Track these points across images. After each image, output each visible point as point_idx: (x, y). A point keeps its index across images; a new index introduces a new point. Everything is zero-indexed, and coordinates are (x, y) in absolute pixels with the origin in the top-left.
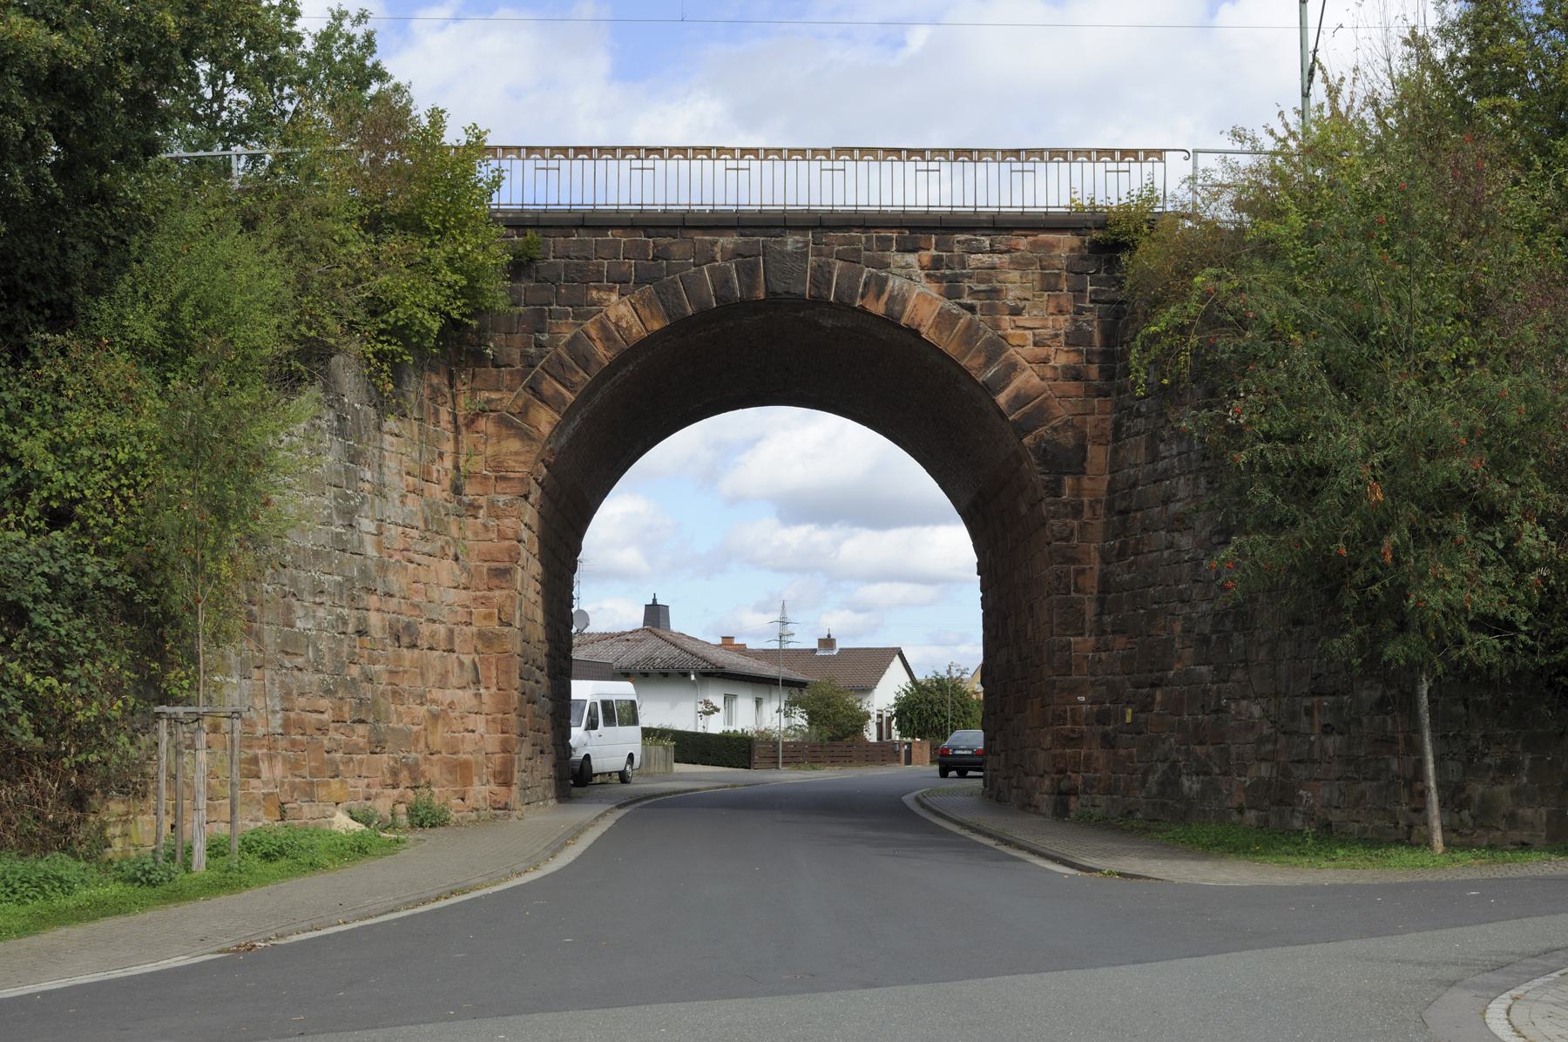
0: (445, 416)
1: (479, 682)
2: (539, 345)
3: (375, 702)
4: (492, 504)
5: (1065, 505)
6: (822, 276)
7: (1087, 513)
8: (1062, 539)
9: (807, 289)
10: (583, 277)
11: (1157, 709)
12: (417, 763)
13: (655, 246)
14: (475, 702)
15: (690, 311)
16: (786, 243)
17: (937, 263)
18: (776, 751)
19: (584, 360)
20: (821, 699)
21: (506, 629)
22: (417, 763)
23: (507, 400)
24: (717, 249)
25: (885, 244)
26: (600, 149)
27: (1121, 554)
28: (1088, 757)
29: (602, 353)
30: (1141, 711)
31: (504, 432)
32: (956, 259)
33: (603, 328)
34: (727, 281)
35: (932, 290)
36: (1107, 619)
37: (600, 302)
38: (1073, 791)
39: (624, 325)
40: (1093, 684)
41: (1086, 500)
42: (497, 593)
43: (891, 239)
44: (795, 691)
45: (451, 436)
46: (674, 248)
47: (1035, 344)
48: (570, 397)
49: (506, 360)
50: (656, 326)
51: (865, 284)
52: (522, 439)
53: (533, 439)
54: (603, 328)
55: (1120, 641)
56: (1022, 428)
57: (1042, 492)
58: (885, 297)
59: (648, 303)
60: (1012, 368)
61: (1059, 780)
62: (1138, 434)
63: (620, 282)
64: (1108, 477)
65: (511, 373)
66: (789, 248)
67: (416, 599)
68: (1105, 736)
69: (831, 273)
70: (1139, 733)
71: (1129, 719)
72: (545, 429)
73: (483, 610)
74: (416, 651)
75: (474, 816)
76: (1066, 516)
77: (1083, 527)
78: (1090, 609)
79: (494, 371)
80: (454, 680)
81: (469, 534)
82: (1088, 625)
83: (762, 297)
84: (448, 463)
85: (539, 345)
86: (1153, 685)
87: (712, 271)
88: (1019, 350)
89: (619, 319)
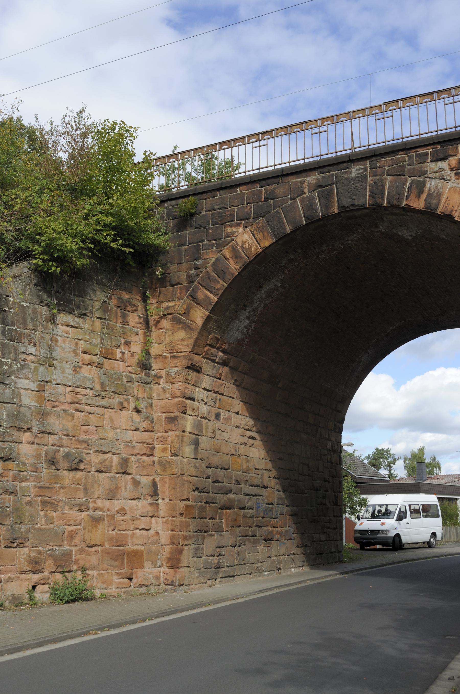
0: (134, 319)
1: (157, 495)
2: (197, 268)
3: (17, 510)
4: (168, 374)
6: (377, 190)
9: (368, 201)
10: (223, 219)
12: (68, 554)
14: (149, 508)
15: (288, 230)
16: (351, 172)
19: (221, 272)
21: (175, 458)
22: (68, 554)
23: (177, 306)
24: (305, 186)
25: (422, 159)
26: (235, 140)
29: (234, 267)
31: (176, 327)
33: (234, 250)
34: (311, 205)
37: (232, 234)
39: (247, 246)
42: (170, 433)
43: (427, 154)
45: (141, 332)
46: (278, 191)
48: (214, 299)
49: (177, 281)
51: (409, 188)
52: (185, 330)
53: (191, 329)
54: (234, 250)
58: (424, 196)
59: (261, 229)
63: (245, 219)
65: (180, 289)
66: (353, 175)
67: (83, 437)
69: (383, 186)
72: (200, 322)
73: (162, 446)
74: (80, 474)
75: (143, 590)
79: (171, 288)
80: (123, 493)
81: (154, 395)
83: (336, 212)
84: (136, 348)
85: (197, 268)
89: (244, 243)
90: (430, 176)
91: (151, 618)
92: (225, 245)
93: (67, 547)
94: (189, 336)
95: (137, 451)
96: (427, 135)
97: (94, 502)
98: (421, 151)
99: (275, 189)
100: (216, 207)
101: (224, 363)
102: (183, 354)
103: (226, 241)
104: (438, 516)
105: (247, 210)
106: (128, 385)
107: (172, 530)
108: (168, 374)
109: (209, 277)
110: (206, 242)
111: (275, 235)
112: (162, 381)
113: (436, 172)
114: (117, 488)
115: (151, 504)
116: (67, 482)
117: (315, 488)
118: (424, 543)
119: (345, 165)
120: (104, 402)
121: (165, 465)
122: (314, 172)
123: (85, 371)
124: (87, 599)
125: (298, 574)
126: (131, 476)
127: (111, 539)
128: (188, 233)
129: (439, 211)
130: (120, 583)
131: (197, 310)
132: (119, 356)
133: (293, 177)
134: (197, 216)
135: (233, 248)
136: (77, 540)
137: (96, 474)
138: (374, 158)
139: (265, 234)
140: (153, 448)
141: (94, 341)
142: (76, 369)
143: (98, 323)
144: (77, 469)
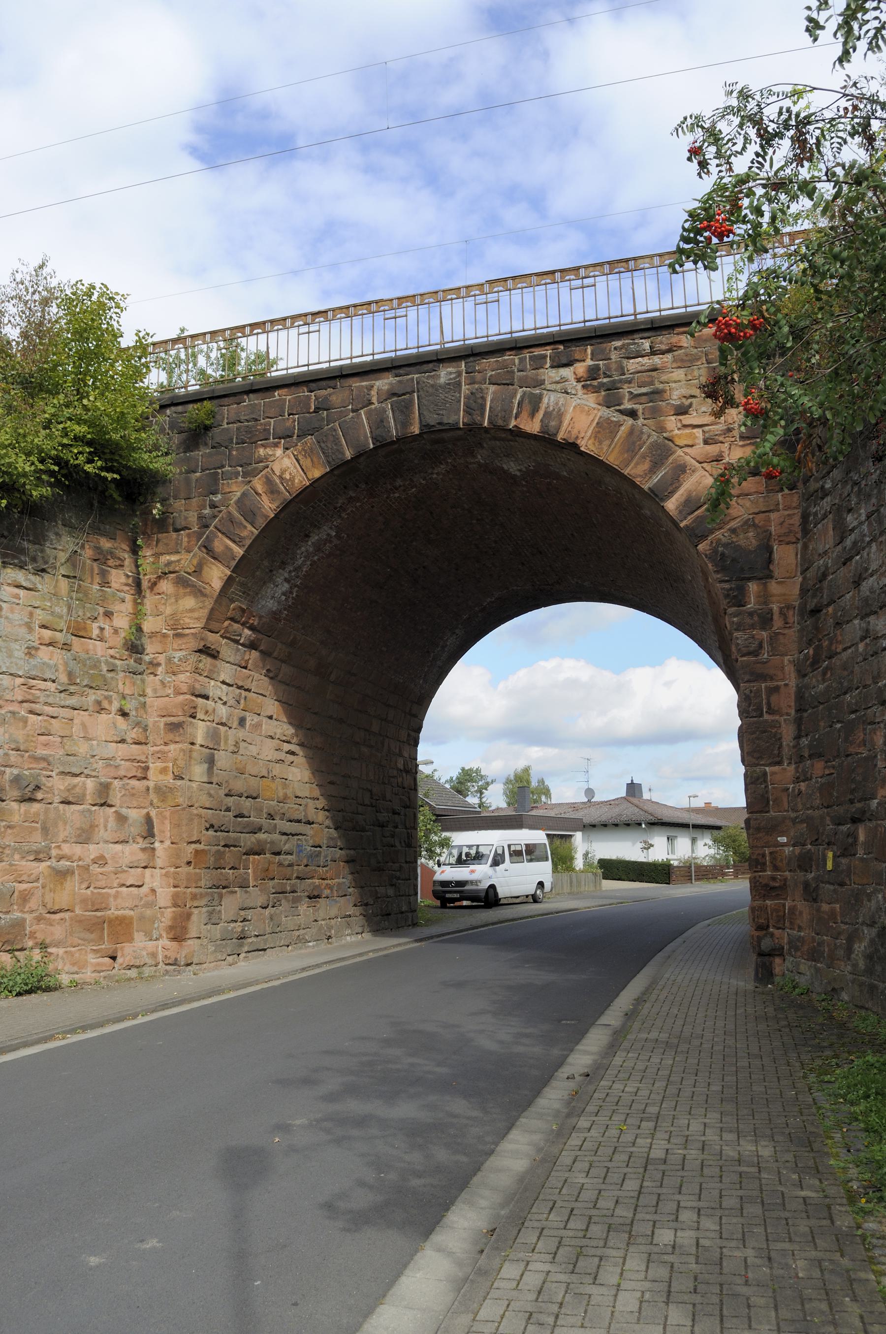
0: (118, 578)
2: (213, 506)
4: (169, 660)
5: (751, 614)
6: (475, 404)
7: (778, 622)
8: (749, 654)
9: (461, 418)
10: (253, 436)
11: (860, 853)
12: (20, 924)
13: (317, 398)
14: (142, 857)
15: (348, 455)
16: (439, 376)
17: (593, 373)
18: (690, 872)
19: (250, 514)
20: (730, 837)
21: (179, 783)
22: (20, 924)
23: (185, 561)
24: (374, 392)
26: (272, 322)
27: (815, 662)
28: (793, 909)
29: (269, 507)
30: (843, 855)
31: (181, 591)
32: (614, 366)
33: (269, 482)
34: (382, 421)
35: (590, 400)
36: (805, 741)
37: (266, 459)
38: (777, 952)
39: (288, 477)
40: (794, 821)
41: (775, 607)
42: (172, 747)
43: (545, 357)
44: (716, 832)
45: (128, 598)
46: (333, 398)
47: (706, 442)
48: (239, 551)
49: (184, 524)
50: (317, 474)
51: (519, 404)
52: (196, 596)
53: (205, 595)
54: (269, 482)
55: (818, 768)
56: (697, 534)
57: (724, 603)
58: (540, 415)
59: (309, 453)
60: (681, 469)
61: (759, 939)
62: (825, 516)
64: (800, 579)
65: (188, 535)
66: (442, 380)
67: (41, 752)
68: (806, 885)
69: (484, 399)
70: (842, 884)
71: (830, 866)
72: (217, 584)
73: (159, 765)
74: (36, 806)
75: (133, 973)
76: (753, 627)
77: (774, 638)
78: (787, 733)
80: (101, 834)
81: (149, 691)
82: (786, 751)
83: (417, 432)
84: (122, 622)
85: (213, 506)
86: (855, 821)
87: (369, 415)
88: (687, 450)
89: (283, 471)
90: (549, 387)
91: (146, 1013)
92: (255, 473)
93: (17, 915)
94: (200, 605)
95: (122, 773)
96: (545, 331)
97: (59, 847)
98: (538, 352)
99: (330, 395)
100: (243, 418)
101: (252, 646)
102: (192, 631)
103: (256, 468)
104: (547, 860)
105: (289, 424)
106: (110, 675)
107: (175, 887)
108: (169, 660)
109: (231, 519)
110: (227, 468)
111: (329, 462)
112: (160, 670)
113: (557, 382)
114: (93, 827)
115: (143, 850)
116: (16, 819)
117: (378, 823)
118: (527, 896)
119: (431, 365)
120: (73, 701)
121: (164, 793)
122: (386, 374)
123: (44, 654)
124: (48, 989)
125: (356, 943)
126: (113, 809)
127: (84, 901)
128: (201, 454)
129: (559, 438)
130: (98, 964)
131: (214, 567)
132: (96, 632)
133: (355, 379)
134: (216, 430)
135: (267, 477)
136: (33, 904)
137: (61, 806)
138: (472, 359)
139: (315, 459)
140: (147, 768)
141: (57, 609)
142: (31, 651)
143: (64, 584)
144: (31, 800)
